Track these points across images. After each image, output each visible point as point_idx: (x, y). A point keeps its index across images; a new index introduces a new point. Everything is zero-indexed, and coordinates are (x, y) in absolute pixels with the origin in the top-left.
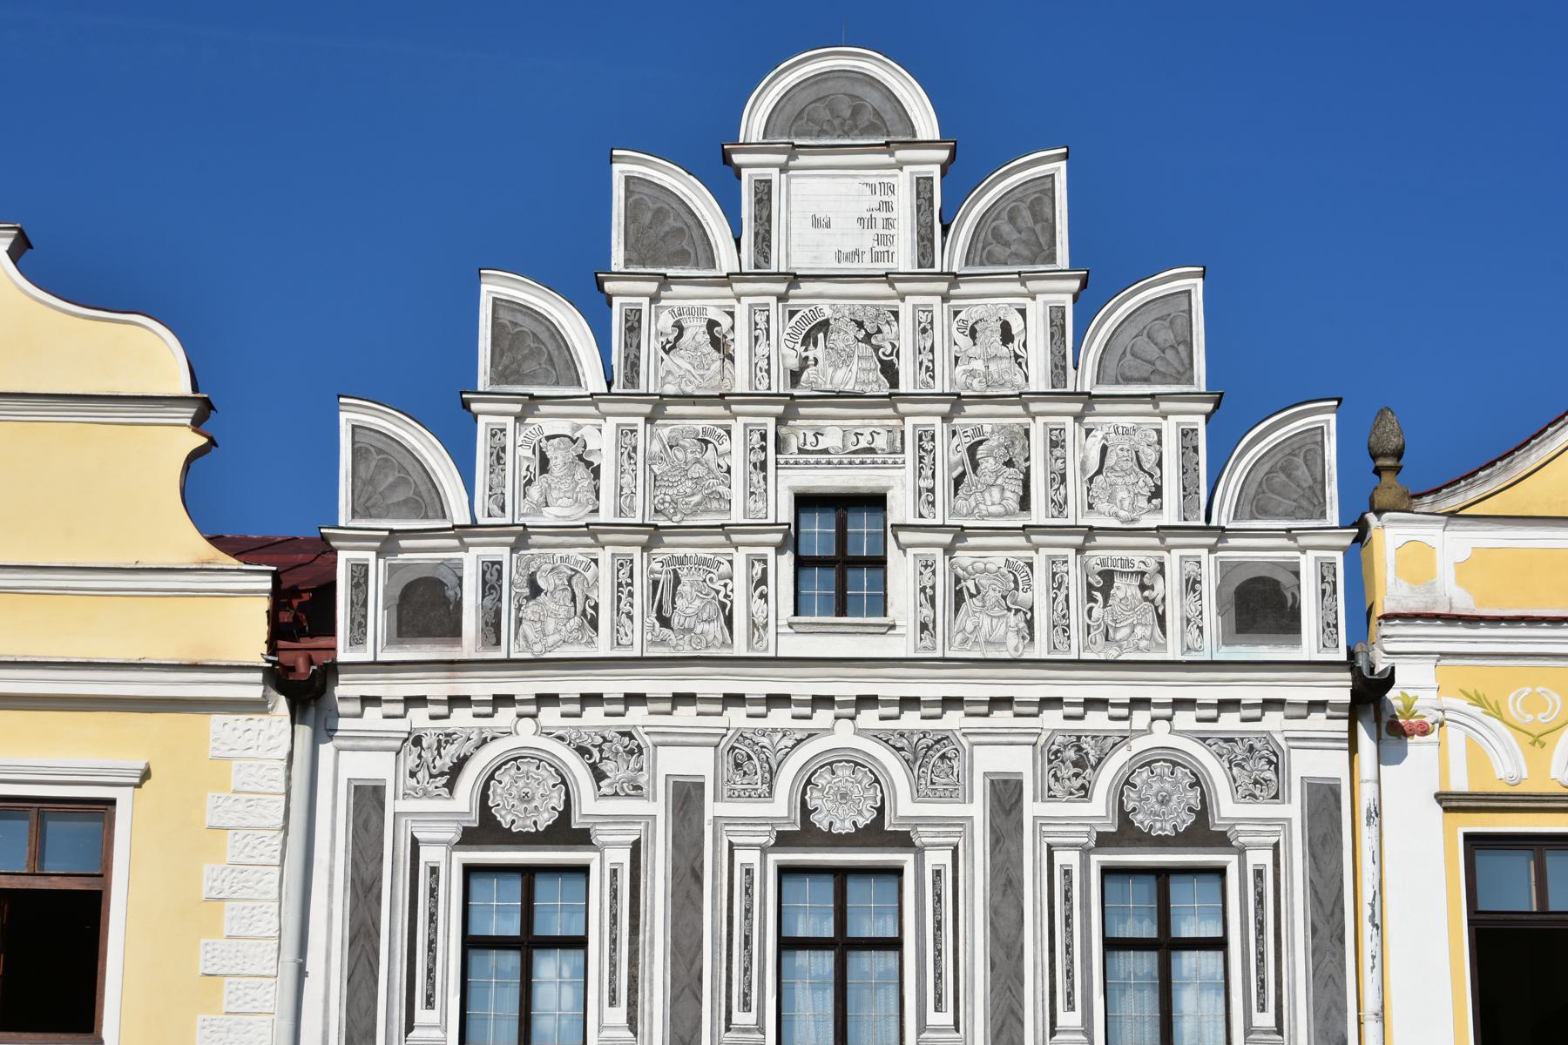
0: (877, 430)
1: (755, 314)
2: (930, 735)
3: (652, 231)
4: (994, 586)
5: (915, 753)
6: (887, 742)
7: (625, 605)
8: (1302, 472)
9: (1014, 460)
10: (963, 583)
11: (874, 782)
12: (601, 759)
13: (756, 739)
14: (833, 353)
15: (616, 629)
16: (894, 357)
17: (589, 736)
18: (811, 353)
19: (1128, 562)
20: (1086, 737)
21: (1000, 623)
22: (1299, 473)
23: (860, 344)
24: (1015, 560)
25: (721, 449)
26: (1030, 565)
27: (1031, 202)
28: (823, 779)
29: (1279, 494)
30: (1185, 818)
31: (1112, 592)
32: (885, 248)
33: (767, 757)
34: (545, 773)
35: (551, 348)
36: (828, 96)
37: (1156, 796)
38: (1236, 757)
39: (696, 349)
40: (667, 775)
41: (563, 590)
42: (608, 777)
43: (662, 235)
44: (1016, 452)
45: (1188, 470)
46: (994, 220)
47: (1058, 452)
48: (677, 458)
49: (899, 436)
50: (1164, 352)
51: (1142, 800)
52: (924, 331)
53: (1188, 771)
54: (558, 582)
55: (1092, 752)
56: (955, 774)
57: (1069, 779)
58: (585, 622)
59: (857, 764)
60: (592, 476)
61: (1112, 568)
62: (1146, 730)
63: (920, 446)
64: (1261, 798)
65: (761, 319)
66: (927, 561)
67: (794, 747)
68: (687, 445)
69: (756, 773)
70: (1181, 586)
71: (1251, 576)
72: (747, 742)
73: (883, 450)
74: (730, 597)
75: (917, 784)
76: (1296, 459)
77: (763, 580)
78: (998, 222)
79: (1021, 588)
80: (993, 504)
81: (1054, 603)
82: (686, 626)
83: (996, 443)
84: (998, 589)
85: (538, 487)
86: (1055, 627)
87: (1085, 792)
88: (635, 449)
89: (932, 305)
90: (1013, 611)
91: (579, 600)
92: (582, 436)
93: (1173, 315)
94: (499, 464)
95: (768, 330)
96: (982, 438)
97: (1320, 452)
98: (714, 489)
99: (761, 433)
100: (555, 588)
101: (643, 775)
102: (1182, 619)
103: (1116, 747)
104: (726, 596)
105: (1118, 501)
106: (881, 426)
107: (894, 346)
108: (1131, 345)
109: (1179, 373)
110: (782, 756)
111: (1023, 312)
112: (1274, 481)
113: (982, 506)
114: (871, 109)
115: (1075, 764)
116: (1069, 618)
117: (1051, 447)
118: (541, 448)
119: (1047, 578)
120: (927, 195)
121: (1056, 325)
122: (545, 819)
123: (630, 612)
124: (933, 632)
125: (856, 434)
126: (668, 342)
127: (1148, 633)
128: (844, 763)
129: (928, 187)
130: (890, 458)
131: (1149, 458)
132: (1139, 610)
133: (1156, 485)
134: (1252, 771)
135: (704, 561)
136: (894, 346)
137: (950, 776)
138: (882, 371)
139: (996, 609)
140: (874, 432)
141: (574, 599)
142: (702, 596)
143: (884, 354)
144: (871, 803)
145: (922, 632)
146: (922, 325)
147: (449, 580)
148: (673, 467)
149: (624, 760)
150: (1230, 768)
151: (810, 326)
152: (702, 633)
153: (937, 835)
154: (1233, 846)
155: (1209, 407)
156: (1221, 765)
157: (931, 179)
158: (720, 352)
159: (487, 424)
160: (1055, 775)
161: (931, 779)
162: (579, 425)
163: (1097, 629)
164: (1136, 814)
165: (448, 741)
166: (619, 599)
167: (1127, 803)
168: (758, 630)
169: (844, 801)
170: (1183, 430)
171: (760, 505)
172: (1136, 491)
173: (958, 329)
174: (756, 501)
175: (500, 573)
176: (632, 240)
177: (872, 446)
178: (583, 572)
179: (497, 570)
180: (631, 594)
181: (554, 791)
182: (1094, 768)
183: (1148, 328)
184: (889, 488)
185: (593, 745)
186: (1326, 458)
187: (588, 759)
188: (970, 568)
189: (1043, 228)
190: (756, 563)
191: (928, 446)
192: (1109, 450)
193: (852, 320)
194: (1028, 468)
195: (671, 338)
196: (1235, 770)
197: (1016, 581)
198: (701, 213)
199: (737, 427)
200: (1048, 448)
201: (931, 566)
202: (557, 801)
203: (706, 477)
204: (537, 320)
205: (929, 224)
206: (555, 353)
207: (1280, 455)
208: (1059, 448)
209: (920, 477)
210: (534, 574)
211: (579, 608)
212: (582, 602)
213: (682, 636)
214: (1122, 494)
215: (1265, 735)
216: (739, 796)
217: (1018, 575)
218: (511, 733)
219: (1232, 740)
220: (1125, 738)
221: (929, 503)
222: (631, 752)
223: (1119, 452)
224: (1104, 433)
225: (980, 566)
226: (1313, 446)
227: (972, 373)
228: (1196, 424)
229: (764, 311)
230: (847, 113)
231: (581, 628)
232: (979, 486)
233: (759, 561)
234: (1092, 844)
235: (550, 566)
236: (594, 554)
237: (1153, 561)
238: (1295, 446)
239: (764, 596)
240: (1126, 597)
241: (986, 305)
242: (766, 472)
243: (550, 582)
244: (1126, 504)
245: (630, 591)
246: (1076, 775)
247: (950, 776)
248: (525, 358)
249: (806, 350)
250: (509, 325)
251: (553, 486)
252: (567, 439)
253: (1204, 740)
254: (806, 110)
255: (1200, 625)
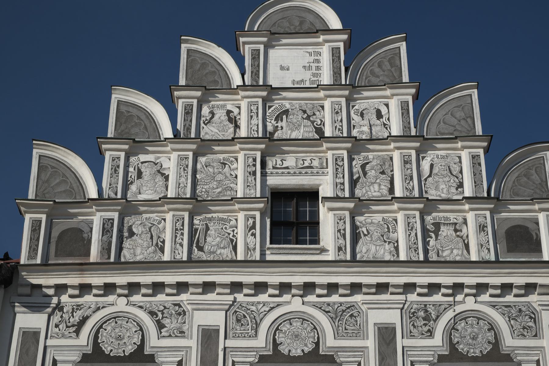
0: (314, 158)
1: (251, 106)
2: (344, 304)
3: (200, 72)
4: (377, 230)
5: (336, 314)
6: (320, 308)
7: (179, 239)
8: (535, 177)
9: (385, 171)
10: (360, 229)
11: (313, 329)
12: (163, 318)
13: (248, 307)
14: (291, 124)
15: (173, 251)
16: (322, 126)
17: (157, 306)
18: (279, 124)
19: (447, 218)
20: (430, 305)
21: (380, 249)
22: (533, 177)
23: (304, 120)
24: (387, 218)
25: (232, 167)
26: (396, 220)
27: (389, 58)
28: (285, 327)
29: (524, 187)
30: (487, 347)
31: (440, 233)
32: (317, 79)
33: (255, 316)
34: (131, 325)
35: (146, 123)
36: (288, 17)
37: (470, 335)
38: (512, 315)
39: (220, 123)
40: (198, 325)
41: (146, 233)
42: (166, 327)
43: (205, 73)
44: (386, 167)
45: (476, 174)
46: (371, 67)
47: (408, 166)
48: (209, 171)
49: (325, 161)
50: (460, 122)
51: (462, 337)
52: (337, 113)
53: (486, 322)
54: (143, 230)
55: (433, 313)
56: (358, 324)
57: (421, 327)
58: (157, 249)
59: (304, 320)
60: (165, 180)
61: (439, 221)
62: (462, 301)
63: (336, 164)
64: (528, 336)
65: (254, 108)
66: (341, 217)
67: (269, 311)
68: (215, 165)
69: (248, 325)
70: (477, 229)
71: (514, 225)
72: (243, 308)
73: (317, 167)
74: (236, 236)
75: (338, 330)
76: (531, 171)
77: (254, 227)
78: (373, 67)
79: (391, 231)
80: (375, 192)
81: (409, 237)
82: (212, 250)
83: (375, 163)
84: (379, 232)
85: (136, 185)
86: (410, 248)
87: (430, 334)
88: (187, 166)
89: (341, 102)
90: (388, 242)
91: (155, 238)
92: (160, 162)
93: (463, 105)
94: (115, 173)
95: (257, 113)
96: (368, 161)
97: (543, 166)
98: (228, 185)
99: (253, 159)
100: (142, 233)
101: (186, 325)
102: (478, 245)
103: (446, 310)
104: (234, 236)
105: (440, 190)
106: (316, 156)
107: (321, 121)
108: (443, 118)
109: (468, 130)
110: (263, 316)
111: (387, 105)
112: (522, 180)
113: (369, 193)
114: (309, 22)
115: (424, 319)
116: (418, 244)
117: (404, 163)
118: (138, 167)
119: (405, 225)
120: (338, 55)
121: (404, 109)
122: (130, 349)
123: (181, 243)
124: (345, 251)
125: (303, 160)
126: (206, 120)
127: (460, 253)
128: (297, 319)
129: (338, 52)
130: (321, 171)
131: (456, 169)
132: (455, 241)
133: (460, 182)
134: (521, 322)
135: (222, 219)
136: (321, 121)
137: (356, 326)
138: (316, 132)
139: (378, 241)
140: (312, 159)
141: (152, 237)
142: (221, 236)
143: (317, 124)
144: (311, 340)
145: (339, 251)
146: (336, 110)
147: (86, 229)
148: (207, 176)
149: (175, 318)
150: (509, 321)
151: (279, 112)
152: (220, 254)
153: (349, 357)
154: (514, 362)
155: (485, 144)
156: (505, 320)
157: (339, 48)
158: (232, 124)
159: (110, 155)
160: (413, 325)
161: (345, 327)
162: (159, 157)
163: (433, 251)
164: (459, 345)
165: (78, 308)
166: (176, 237)
167: (454, 339)
168: (250, 251)
169: (297, 339)
170: (472, 155)
171: (252, 191)
172: (450, 185)
173: (354, 113)
174: (250, 190)
175: (112, 224)
176: (190, 76)
177: (311, 165)
178: (157, 225)
179: (111, 223)
180: (182, 234)
181: (135, 334)
182: (435, 321)
183: (451, 111)
184: (320, 185)
185: (159, 311)
186: (547, 171)
187: (155, 318)
188: (364, 222)
189: (395, 69)
190: (250, 219)
191: (341, 164)
192: (434, 166)
193: (300, 110)
194: (393, 175)
195: (208, 118)
196: (512, 322)
197: (388, 228)
198: (225, 65)
199: (241, 156)
200: (403, 164)
201: (343, 219)
202: (137, 339)
203: (224, 180)
204: (140, 110)
205: (339, 67)
206: (148, 125)
207: (522, 169)
208: (409, 164)
209: (336, 177)
210: (131, 226)
211: (155, 242)
212: (156, 239)
213: (209, 256)
214: (442, 186)
215: (527, 304)
216: (239, 337)
217: (389, 225)
218: (113, 305)
219: (509, 306)
220: (451, 305)
221: (341, 189)
222: (179, 314)
223: (440, 166)
224: (431, 158)
225: (369, 221)
226: (539, 165)
227: (362, 132)
228: (479, 152)
229: (255, 105)
230: (297, 24)
231: (155, 252)
232: (367, 183)
233: (251, 218)
234: (436, 361)
235: (140, 222)
236: (164, 216)
237: (461, 218)
238: (530, 165)
239: (254, 235)
240: (447, 235)
241: (368, 102)
242: (256, 176)
243: (140, 230)
244: (445, 191)
245: (182, 232)
246: (425, 325)
247: (356, 326)
248: (132, 126)
249: (277, 123)
250: (125, 112)
251: (144, 185)
252: (152, 163)
253: (494, 306)
254: (277, 23)
255: (488, 248)
